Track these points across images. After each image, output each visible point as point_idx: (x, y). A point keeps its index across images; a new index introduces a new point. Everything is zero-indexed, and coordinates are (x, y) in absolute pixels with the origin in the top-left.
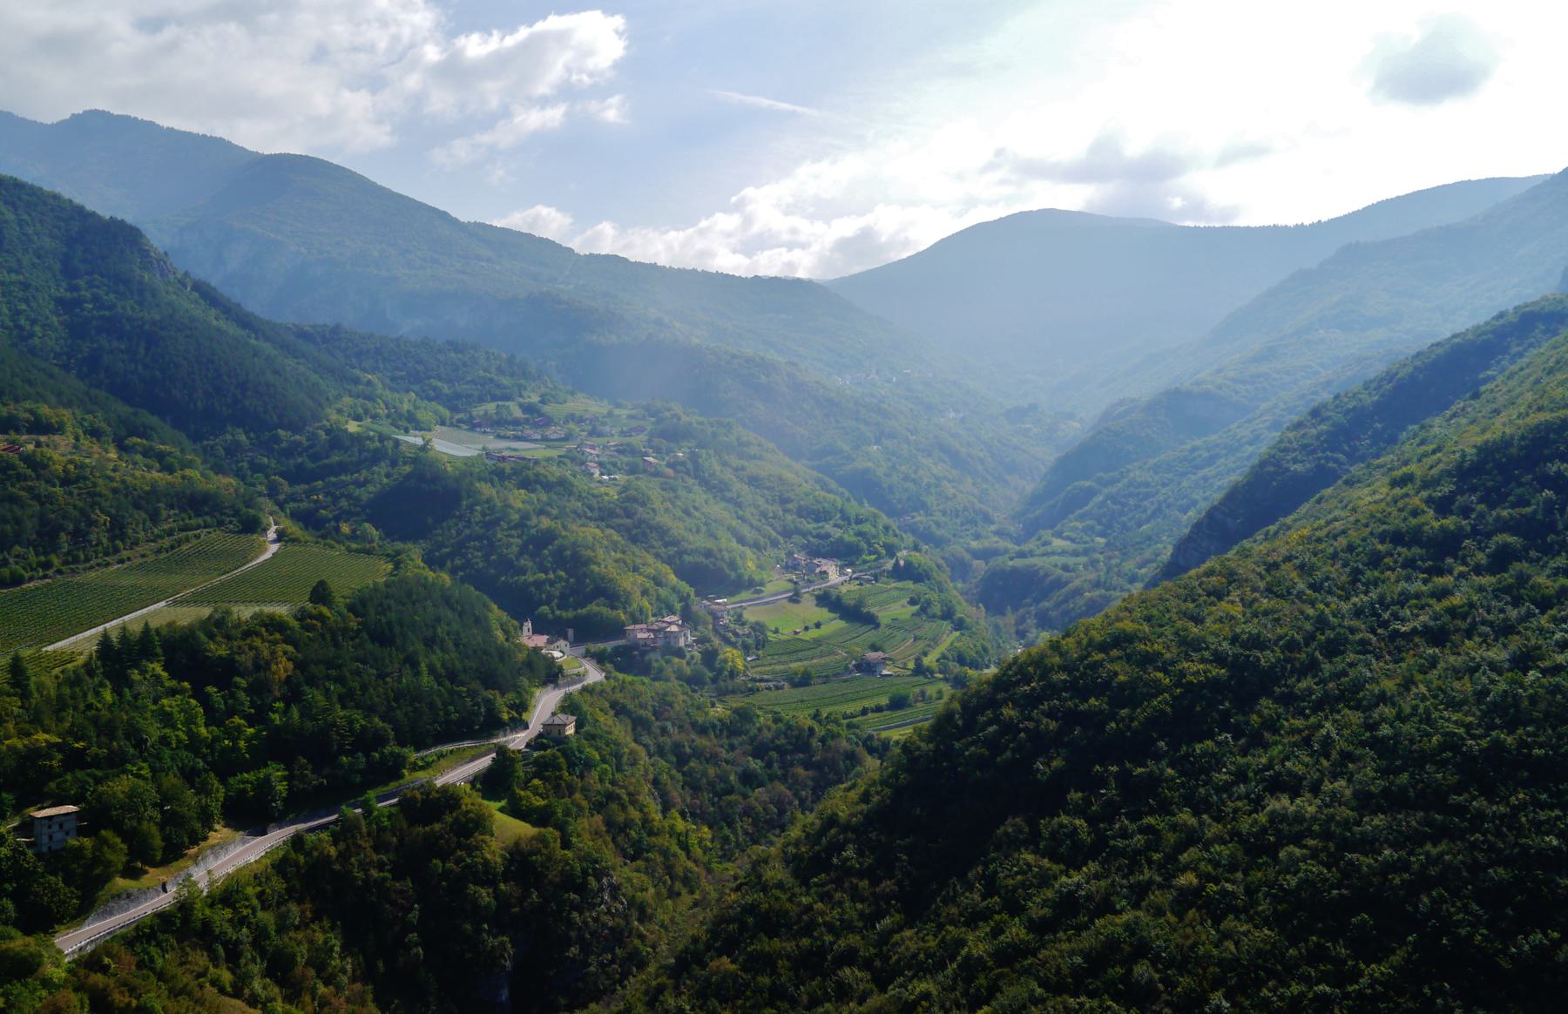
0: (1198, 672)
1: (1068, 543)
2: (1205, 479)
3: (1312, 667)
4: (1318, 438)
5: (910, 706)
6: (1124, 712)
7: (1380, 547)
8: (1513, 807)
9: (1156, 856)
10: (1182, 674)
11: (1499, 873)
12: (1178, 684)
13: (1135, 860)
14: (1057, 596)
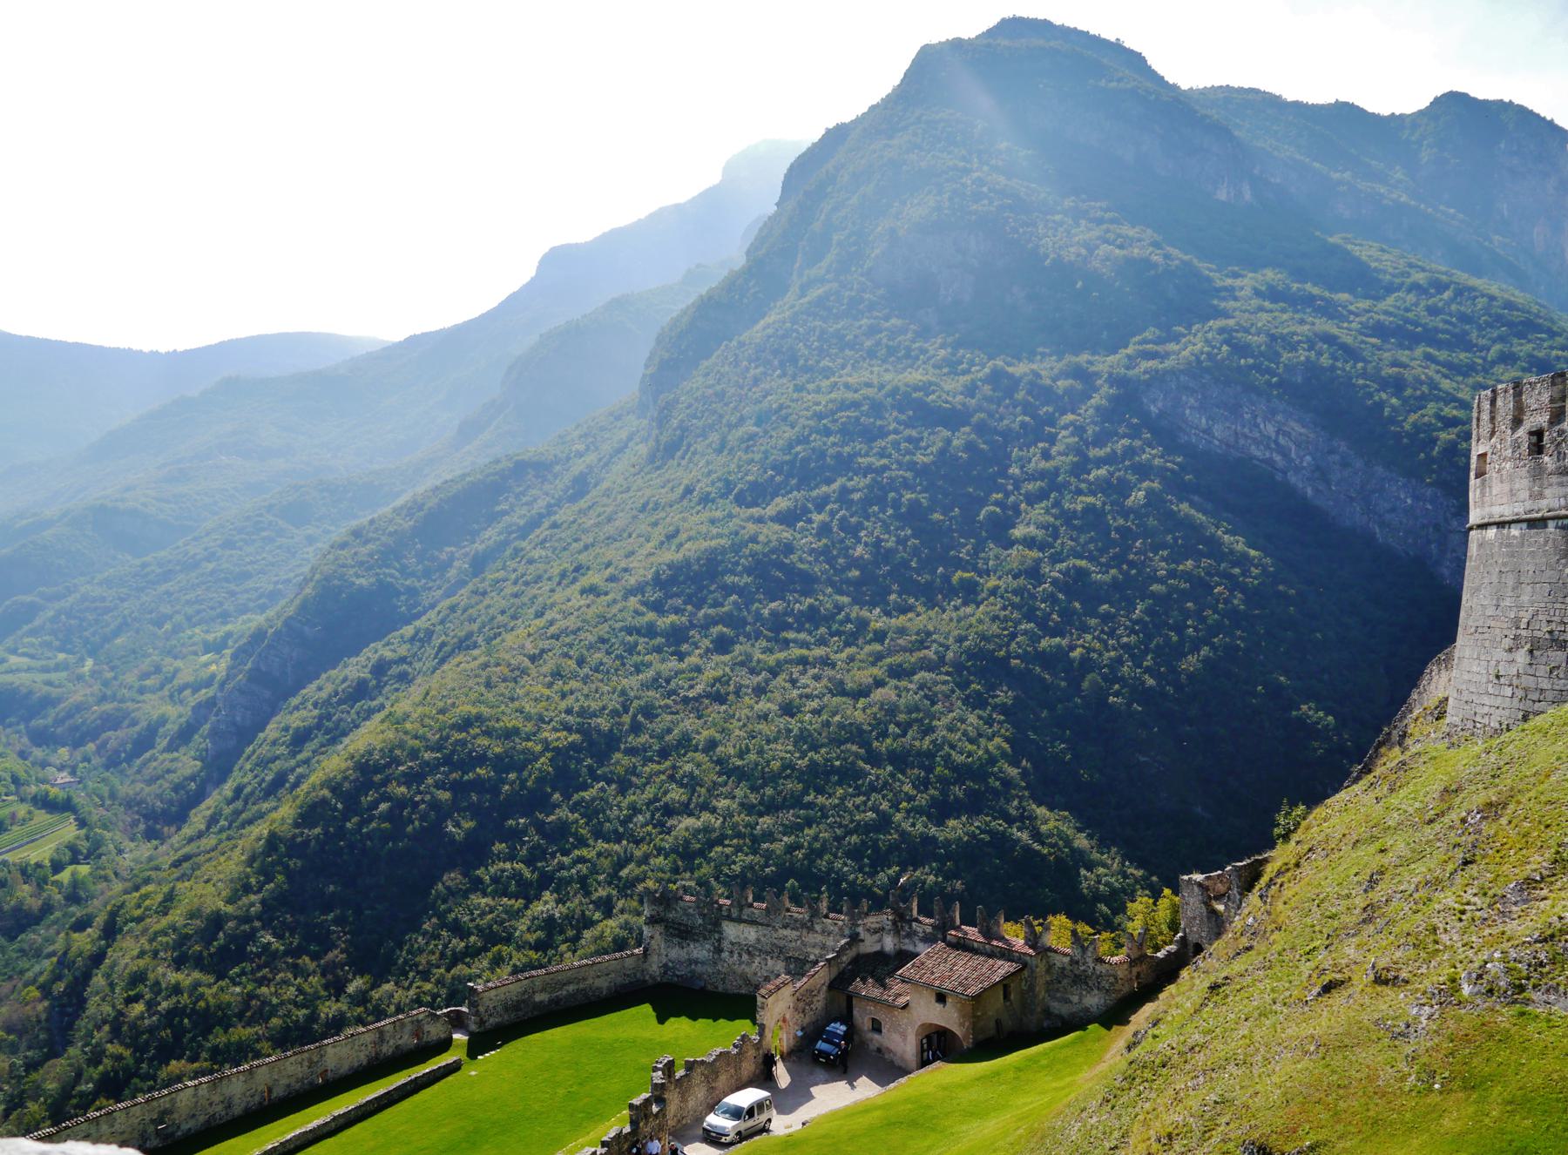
0: (559, 738)
1: (25, 660)
2: (168, 593)
3: (636, 728)
4: (371, 555)
5: (6, 830)
6: (512, 776)
7: (629, 638)
8: (840, 798)
9: (601, 878)
10: (546, 742)
11: (854, 839)
12: (547, 749)
13: (584, 884)
14: (52, 713)
